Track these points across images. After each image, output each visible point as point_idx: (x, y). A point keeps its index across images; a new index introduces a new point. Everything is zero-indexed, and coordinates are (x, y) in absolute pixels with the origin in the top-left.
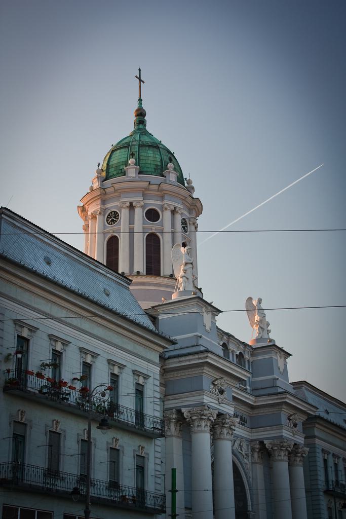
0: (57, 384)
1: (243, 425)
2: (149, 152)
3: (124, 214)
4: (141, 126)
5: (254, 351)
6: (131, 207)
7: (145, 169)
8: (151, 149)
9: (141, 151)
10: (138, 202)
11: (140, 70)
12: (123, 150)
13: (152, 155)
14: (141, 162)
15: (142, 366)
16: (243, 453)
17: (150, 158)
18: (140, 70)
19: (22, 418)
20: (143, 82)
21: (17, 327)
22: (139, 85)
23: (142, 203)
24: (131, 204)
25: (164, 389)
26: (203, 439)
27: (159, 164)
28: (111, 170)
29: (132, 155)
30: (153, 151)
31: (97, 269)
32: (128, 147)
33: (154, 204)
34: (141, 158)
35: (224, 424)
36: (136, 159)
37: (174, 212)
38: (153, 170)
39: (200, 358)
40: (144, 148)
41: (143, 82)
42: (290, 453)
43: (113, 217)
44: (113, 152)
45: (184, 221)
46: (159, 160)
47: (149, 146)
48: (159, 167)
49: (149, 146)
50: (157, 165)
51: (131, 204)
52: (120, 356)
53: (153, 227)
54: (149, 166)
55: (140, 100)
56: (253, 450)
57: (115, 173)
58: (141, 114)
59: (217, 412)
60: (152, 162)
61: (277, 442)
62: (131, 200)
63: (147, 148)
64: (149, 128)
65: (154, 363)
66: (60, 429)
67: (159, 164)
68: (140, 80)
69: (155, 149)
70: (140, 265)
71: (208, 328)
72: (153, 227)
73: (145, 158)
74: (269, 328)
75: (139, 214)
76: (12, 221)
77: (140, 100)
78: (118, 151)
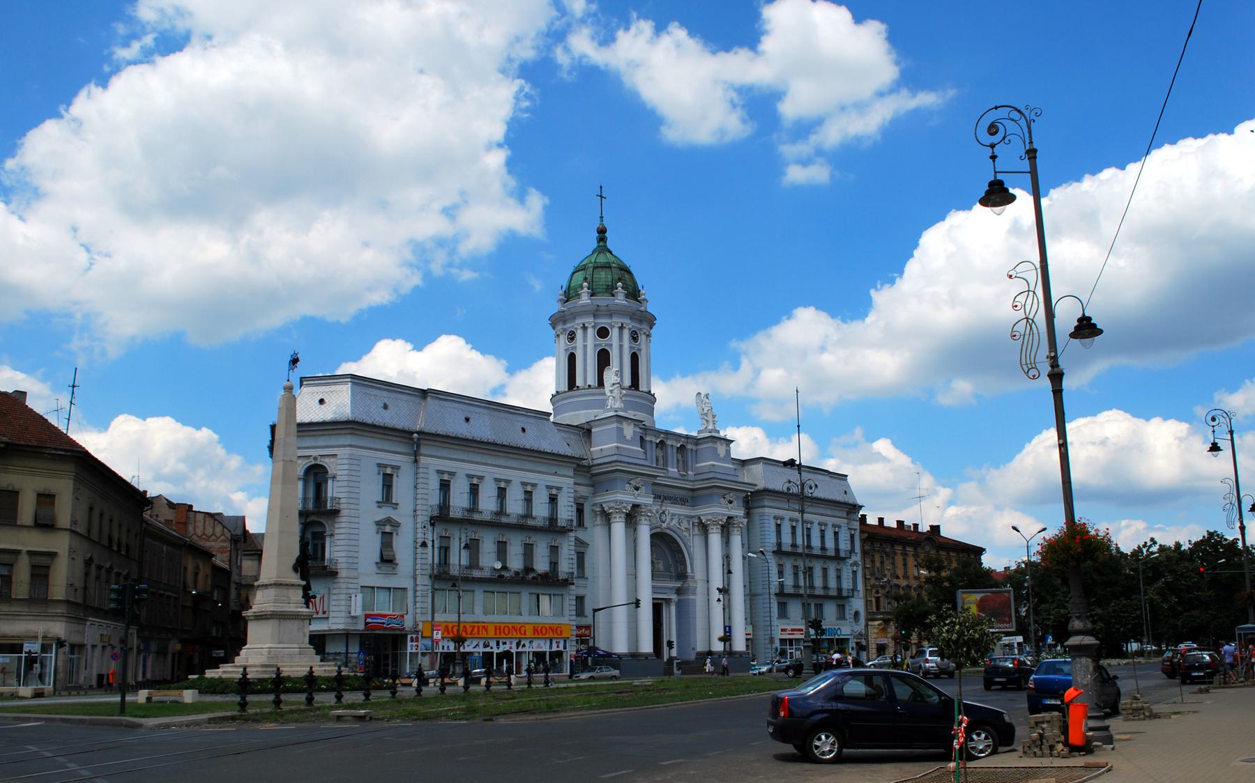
1: (684, 505)
2: (602, 273)
3: (579, 334)
4: (601, 244)
5: (697, 441)
6: (585, 328)
7: (598, 290)
8: (604, 270)
9: (595, 273)
10: (590, 323)
11: (601, 187)
12: (580, 273)
13: (604, 276)
14: (594, 284)
15: (555, 481)
16: (682, 528)
18: (601, 187)
20: (605, 198)
21: (440, 475)
22: (600, 202)
23: (593, 324)
24: (584, 324)
25: (592, 488)
27: (610, 284)
28: (571, 292)
30: (606, 272)
32: (584, 269)
33: (603, 322)
34: (594, 280)
35: (642, 512)
37: (621, 328)
38: (605, 290)
39: (612, 467)
40: (597, 270)
41: (605, 198)
42: (722, 526)
43: (572, 337)
44: (574, 273)
47: (602, 267)
48: (610, 287)
49: (602, 267)
50: (608, 286)
51: (584, 324)
52: (531, 477)
53: (603, 342)
54: (601, 287)
55: (602, 217)
58: (602, 232)
59: (631, 505)
60: (604, 283)
61: (710, 517)
63: (600, 270)
64: (610, 245)
67: (610, 284)
68: (601, 197)
69: (608, 270)
71: (629, 437)
74: (716, 419)
77: (602, 217)
78: (577, 274)
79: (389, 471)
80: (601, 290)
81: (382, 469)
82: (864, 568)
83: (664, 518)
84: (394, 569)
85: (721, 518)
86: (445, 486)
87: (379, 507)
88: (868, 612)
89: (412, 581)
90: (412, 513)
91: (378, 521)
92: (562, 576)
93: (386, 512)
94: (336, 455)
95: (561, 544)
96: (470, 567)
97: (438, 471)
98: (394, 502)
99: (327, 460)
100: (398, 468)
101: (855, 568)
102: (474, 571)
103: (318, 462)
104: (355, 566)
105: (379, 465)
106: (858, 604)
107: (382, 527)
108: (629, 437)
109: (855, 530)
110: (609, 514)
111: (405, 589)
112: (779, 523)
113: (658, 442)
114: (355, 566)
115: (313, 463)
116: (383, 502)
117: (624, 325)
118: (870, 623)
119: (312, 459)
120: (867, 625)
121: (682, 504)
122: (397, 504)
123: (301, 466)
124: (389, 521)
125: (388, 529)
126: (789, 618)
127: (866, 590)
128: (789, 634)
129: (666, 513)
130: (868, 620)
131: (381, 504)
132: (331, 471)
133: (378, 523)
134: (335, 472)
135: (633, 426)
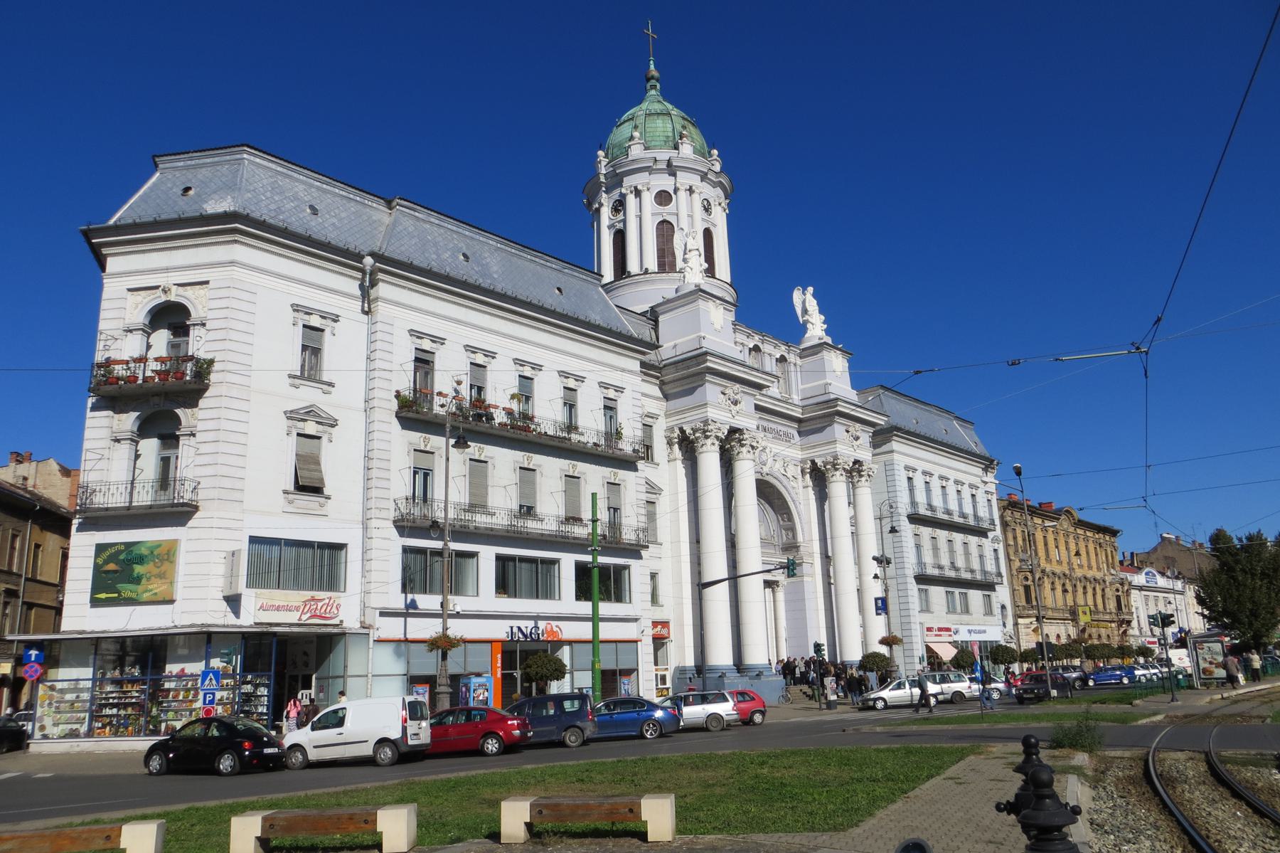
0: (480, 408)
3: (631, 201)
7: (653, 143)
8: (661, 117)
13: (661, 125)
16: (789, 475)
17: (659, 129)
19: (426, 446)
26: (710, 461)
27: (670, 134)
29: (636, 127)
31: (548, 264)
32: (632, 119)
34: (648, 130)
36: (641, 134)
40: (651, 118)
45: (705, 203)
46: (671, 130)
47: (658, 114)
49: (658, 114)
50: (668, 137)
54: (658, 139)
56: (803, 471)
57: (618, 153)
60: (661, 134)
62: (634, 184)
63: (656, 117)
65: (631, 372)
66: (485, 456)
70: (652, 263)
72: (667, 212)
73: (651, 130)
75: (648, 198)
76: (412, 212)
79: (315, 321)
80: (657, 143)
81: (301, 315)
82: (1007, 546)
83: (764, 458)
84: (322, 506)
85: (846, 459)
86: (423, 363)
87: (293, 385)
88: (1015, 606)
89: (359, 532)
90: (362, 405)
91: (291, 411)
92: (628, 536)
93: (308, 395)
94: (207, 282)
95: (624, 481)
96: (472, 508)
97: (412, 332)
98: (325, 379)
99: (189, 292)
100: (336, 319)
101: (996, 546)
102: (478, 515)
103: (173, 298)
104: (237, 495)
105: (296, 308)
106: (1002, 594)
107: (300, 424)
108: (718, 326)
109: (992, 494)
110: (692, 442)
111: (340, 547)
112: (911, 476)
113: (751, 346)
114: (237, 495)
115: (163, 298)
116: (301, 377)
117: (694, 188)
118: (1020, 621)
119: (159, 292)
120: (1016, 624)
121: (786, 441)
122: (331, 385)
123: (140, 306)
124: (310, 413)
125: (311, 428)
126: (932, 613)
127: (1012, 575)
128: (936, 635)
129: (767, 450)
130: (1017, 616)
131: (298, 382)
132: (196, 314)
133: (292, 415)
134: (204, 315)
135: (722, 309)
